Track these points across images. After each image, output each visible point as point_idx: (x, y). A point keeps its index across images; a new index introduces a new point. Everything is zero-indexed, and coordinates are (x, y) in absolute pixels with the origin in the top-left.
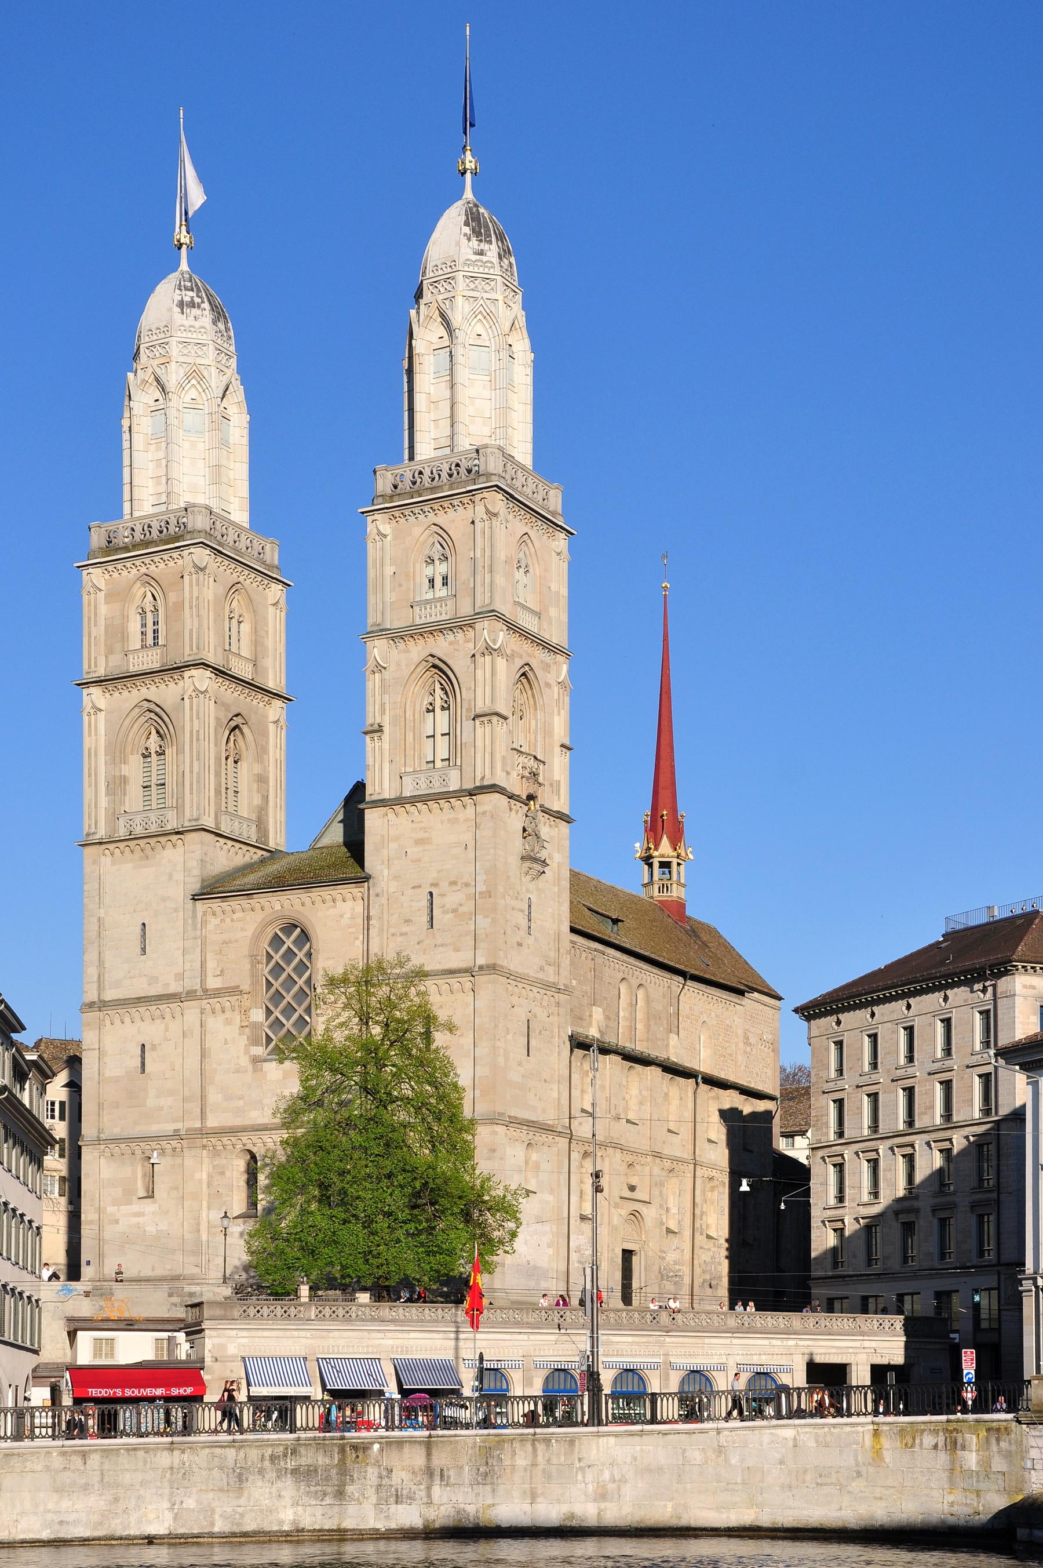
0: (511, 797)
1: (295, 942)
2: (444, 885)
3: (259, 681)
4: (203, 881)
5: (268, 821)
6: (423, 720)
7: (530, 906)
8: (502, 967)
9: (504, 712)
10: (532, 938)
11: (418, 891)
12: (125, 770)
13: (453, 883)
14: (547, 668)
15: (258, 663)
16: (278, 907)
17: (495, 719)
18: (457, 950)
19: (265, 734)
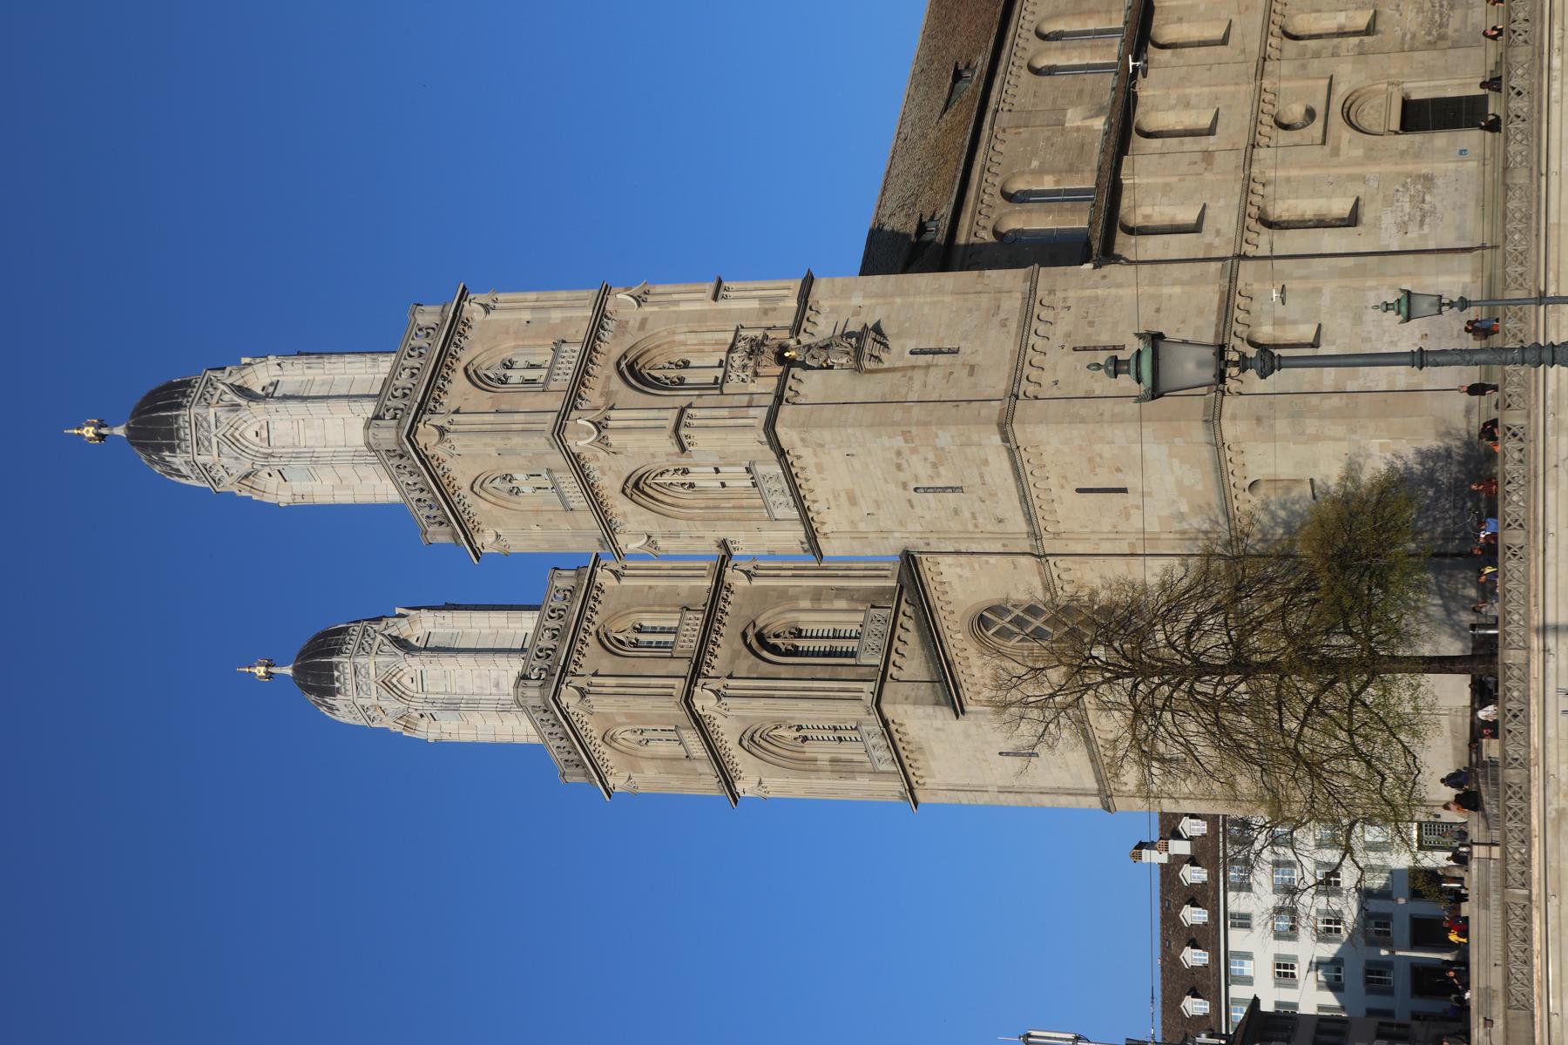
0: (779, 399)
1: (1001, 616)
2: (902, 476)
3: (705, 598)
4: (937, 703)
5: (866, 589)
6: (703, 490)
7: (923, 352)
8: (1002, 410)
9: (672, 415)
10: (966, 347)
11: (915, 502)
12: (823, 762)
13: (899, 467)
14: (623, 325)
15: (685, 603)
16: (959, 636)
17: (683, 432)
18: (986, 462)
19: (764, 591)
